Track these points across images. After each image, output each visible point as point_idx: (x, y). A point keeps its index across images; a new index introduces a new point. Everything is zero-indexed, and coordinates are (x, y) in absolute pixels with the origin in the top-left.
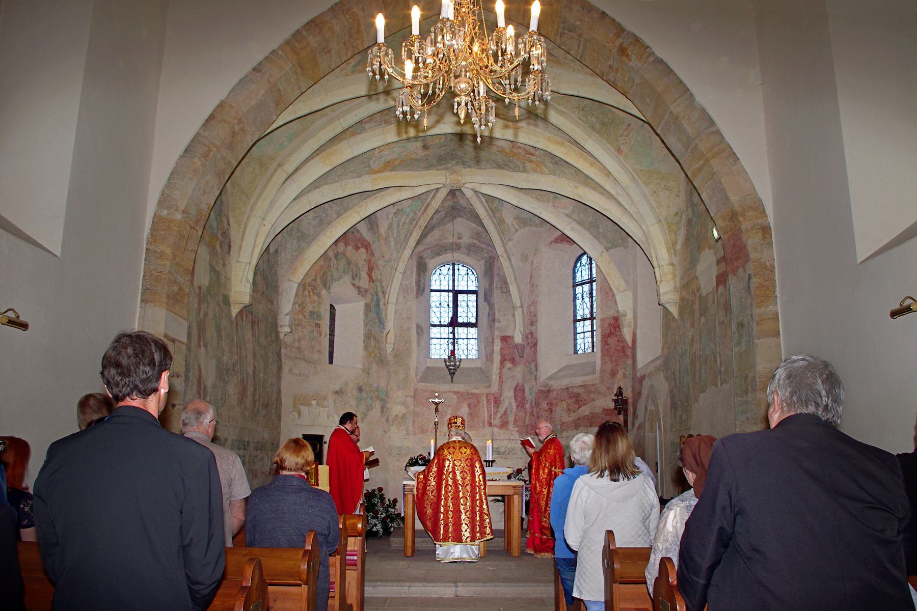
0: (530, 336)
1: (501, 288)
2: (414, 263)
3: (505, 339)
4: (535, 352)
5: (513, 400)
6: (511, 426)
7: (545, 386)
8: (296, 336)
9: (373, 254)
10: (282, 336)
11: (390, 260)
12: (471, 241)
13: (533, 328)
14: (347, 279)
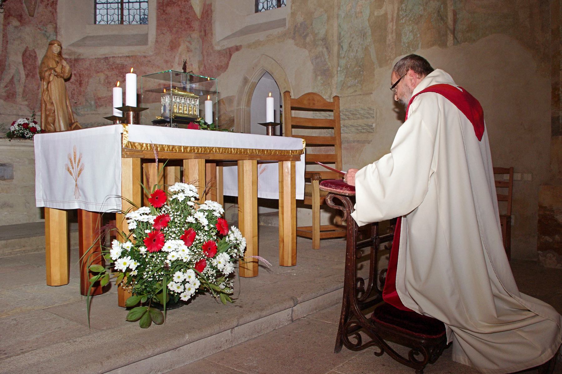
4: (54, 13)
5: (22, 66)
6: (19, 99)
7: (70, 54)
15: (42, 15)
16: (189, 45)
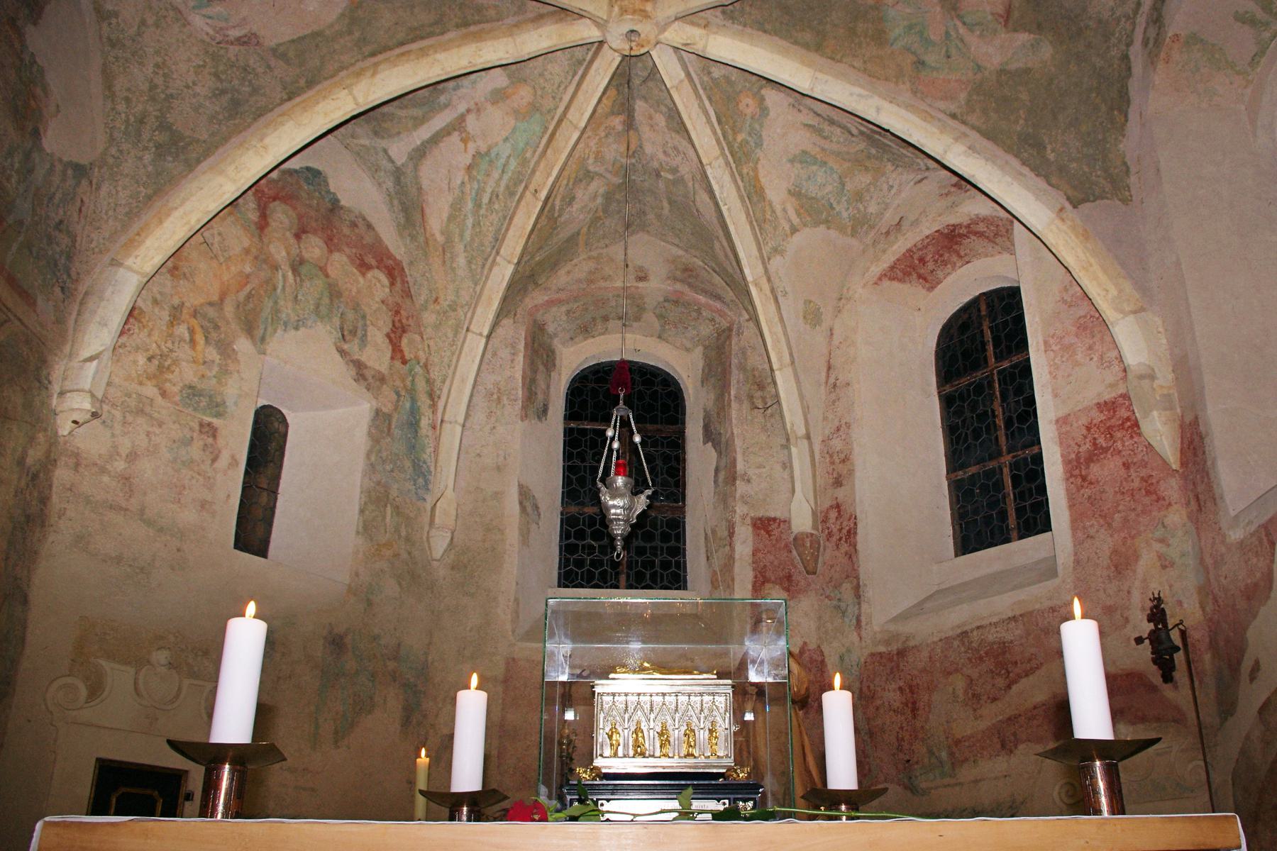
0: (833, 514)
1: (751, 397)
2: (515, 332)
3: (764, 525)
4: (852, 555)
7: (887, 642)
8: (125, 446)
9: (407, 294)
10: (65, 427)
11: (453, 307)
12: (669, 287)
13: (841, 493)
14: (323, 335)
15: (832, 566)
16: (1163, 549)
